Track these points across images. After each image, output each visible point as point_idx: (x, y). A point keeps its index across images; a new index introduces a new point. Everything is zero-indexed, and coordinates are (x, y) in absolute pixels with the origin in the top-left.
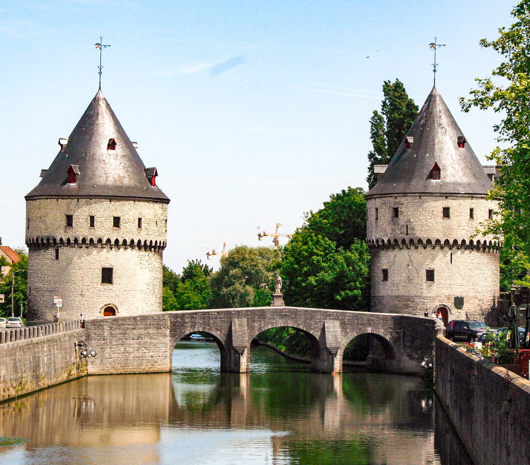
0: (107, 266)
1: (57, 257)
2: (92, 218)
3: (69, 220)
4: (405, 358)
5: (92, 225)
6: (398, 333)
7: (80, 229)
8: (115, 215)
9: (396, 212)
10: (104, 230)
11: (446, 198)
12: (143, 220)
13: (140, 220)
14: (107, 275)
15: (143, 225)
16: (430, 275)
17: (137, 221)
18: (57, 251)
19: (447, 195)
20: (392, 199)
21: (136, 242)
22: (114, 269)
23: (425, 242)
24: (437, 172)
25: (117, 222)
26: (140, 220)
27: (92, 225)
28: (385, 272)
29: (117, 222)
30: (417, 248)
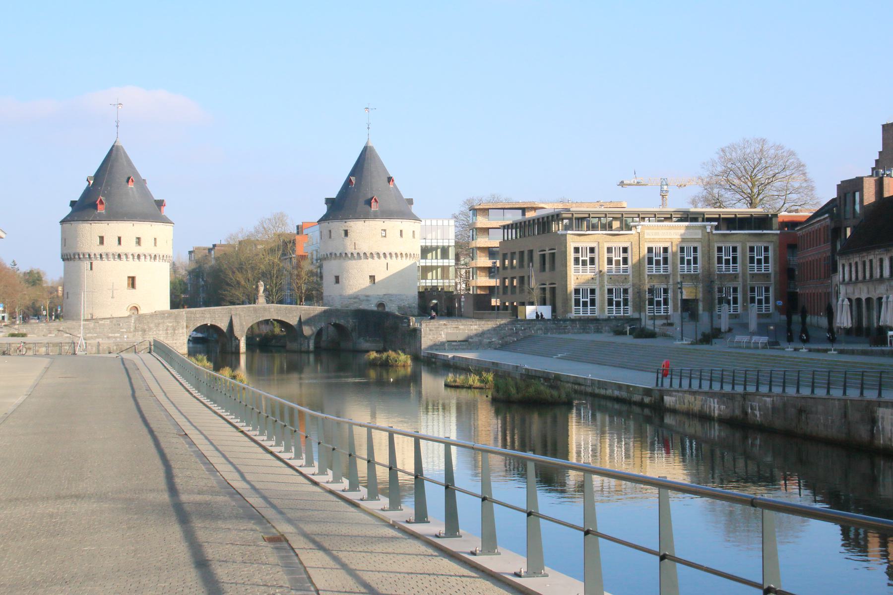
1: (91, 269)
2: (119, 239)
3: (102, 239)
4: (361, 340)
5: (120, 243)
7: (111, 246)
9: (346, 233)
14: (132, 282)
18: (91, 264)
25: (139, 241)
27: (120, 243)
29: (139, 241)
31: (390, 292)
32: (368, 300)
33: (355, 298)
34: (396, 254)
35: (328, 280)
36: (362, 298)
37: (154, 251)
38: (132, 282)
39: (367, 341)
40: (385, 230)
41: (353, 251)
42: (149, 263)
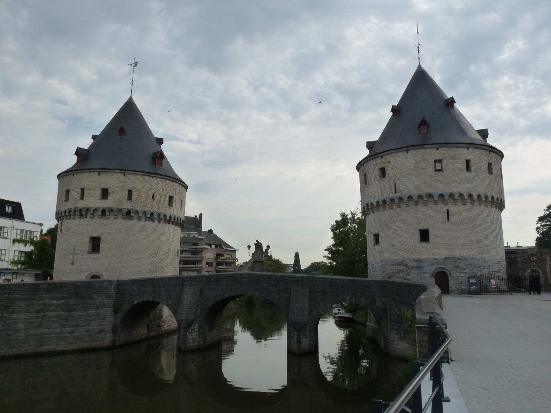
0: (95, 235)
6: (383, 302)
8: (103, 187)
9: (383, 172)
10: (93, 200)
11: (437, 149)
12: (133, 192)
13: (130, 192)
14: (95, 244)
15: (134, 197)
16: (424, 236)
17: (127, 193)
19: (438, 145)
20: (379, 160)
21: (125, 211)
22: (102, 239)
23: (415, 198)
24: (426, 127)
25: (105, 193)
26: (130, 192)
28: (376, 236)
29: (105, 193)
30: (408, 206)
31: (455, 254)
32: (419, 267)
33: (400, 264)
34: (461, 195)
35: (370, 240)
36: (410, 264)
37: (126, 206)
38: (95, 244)
39: (402, 339)
40: (440, 161)
41: (393, 195)
42: (121, 222)
